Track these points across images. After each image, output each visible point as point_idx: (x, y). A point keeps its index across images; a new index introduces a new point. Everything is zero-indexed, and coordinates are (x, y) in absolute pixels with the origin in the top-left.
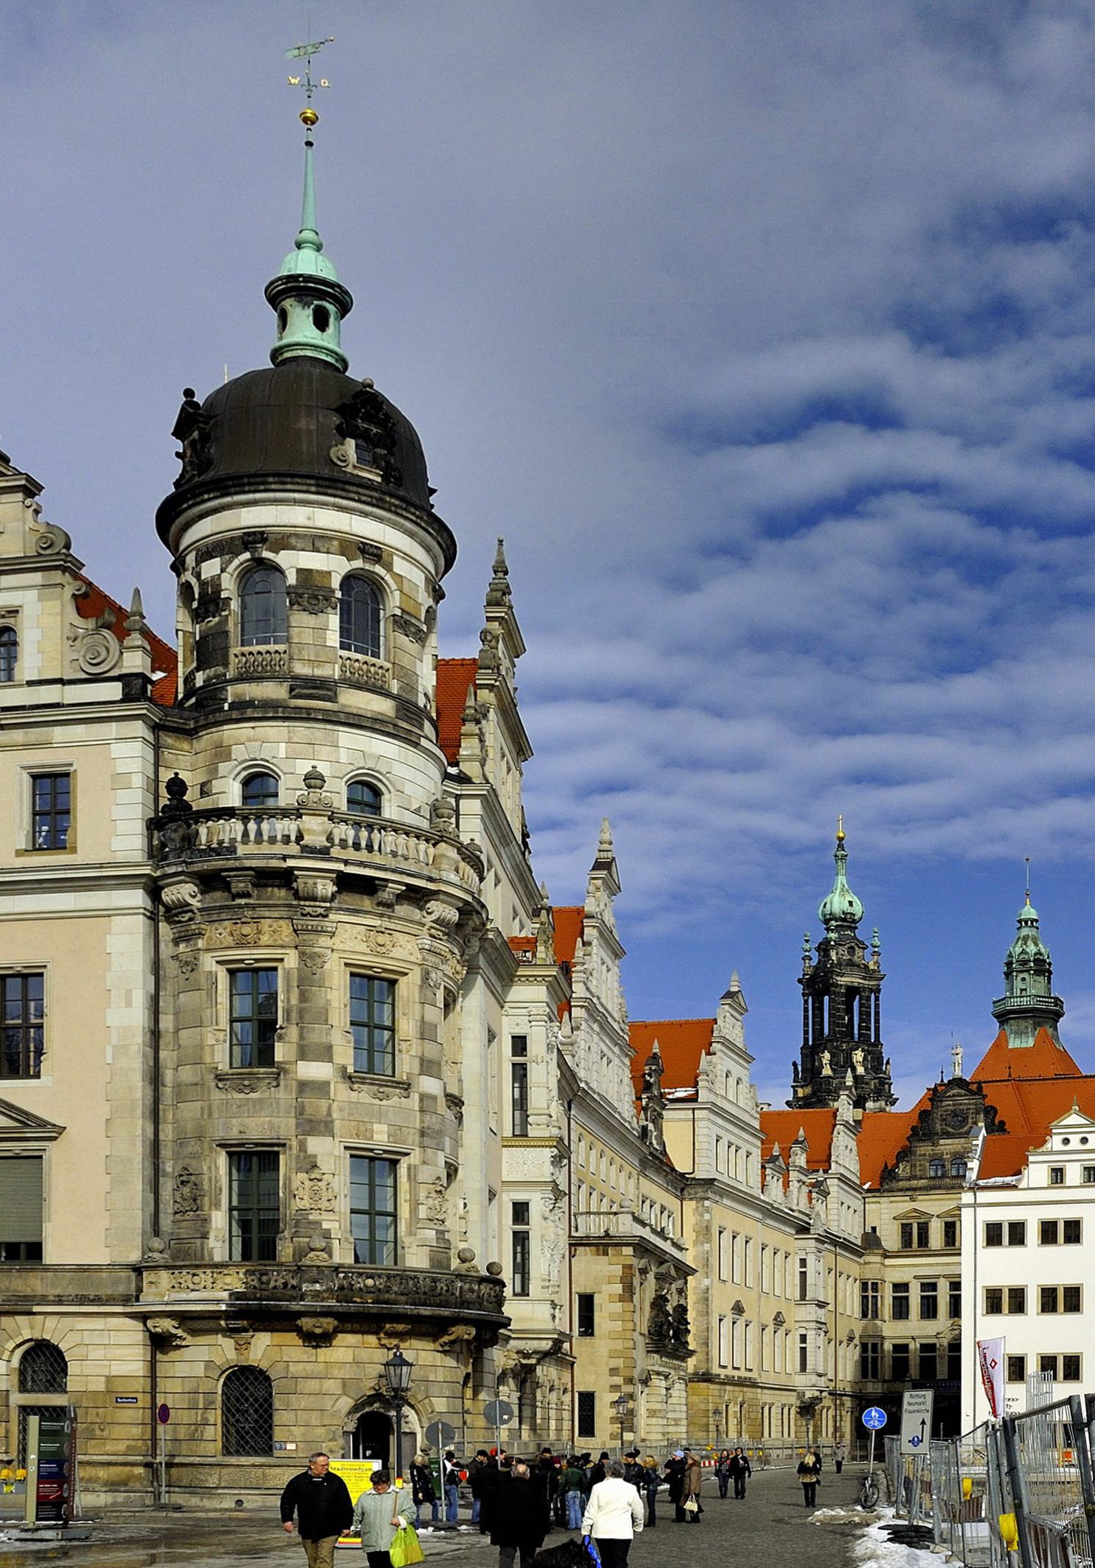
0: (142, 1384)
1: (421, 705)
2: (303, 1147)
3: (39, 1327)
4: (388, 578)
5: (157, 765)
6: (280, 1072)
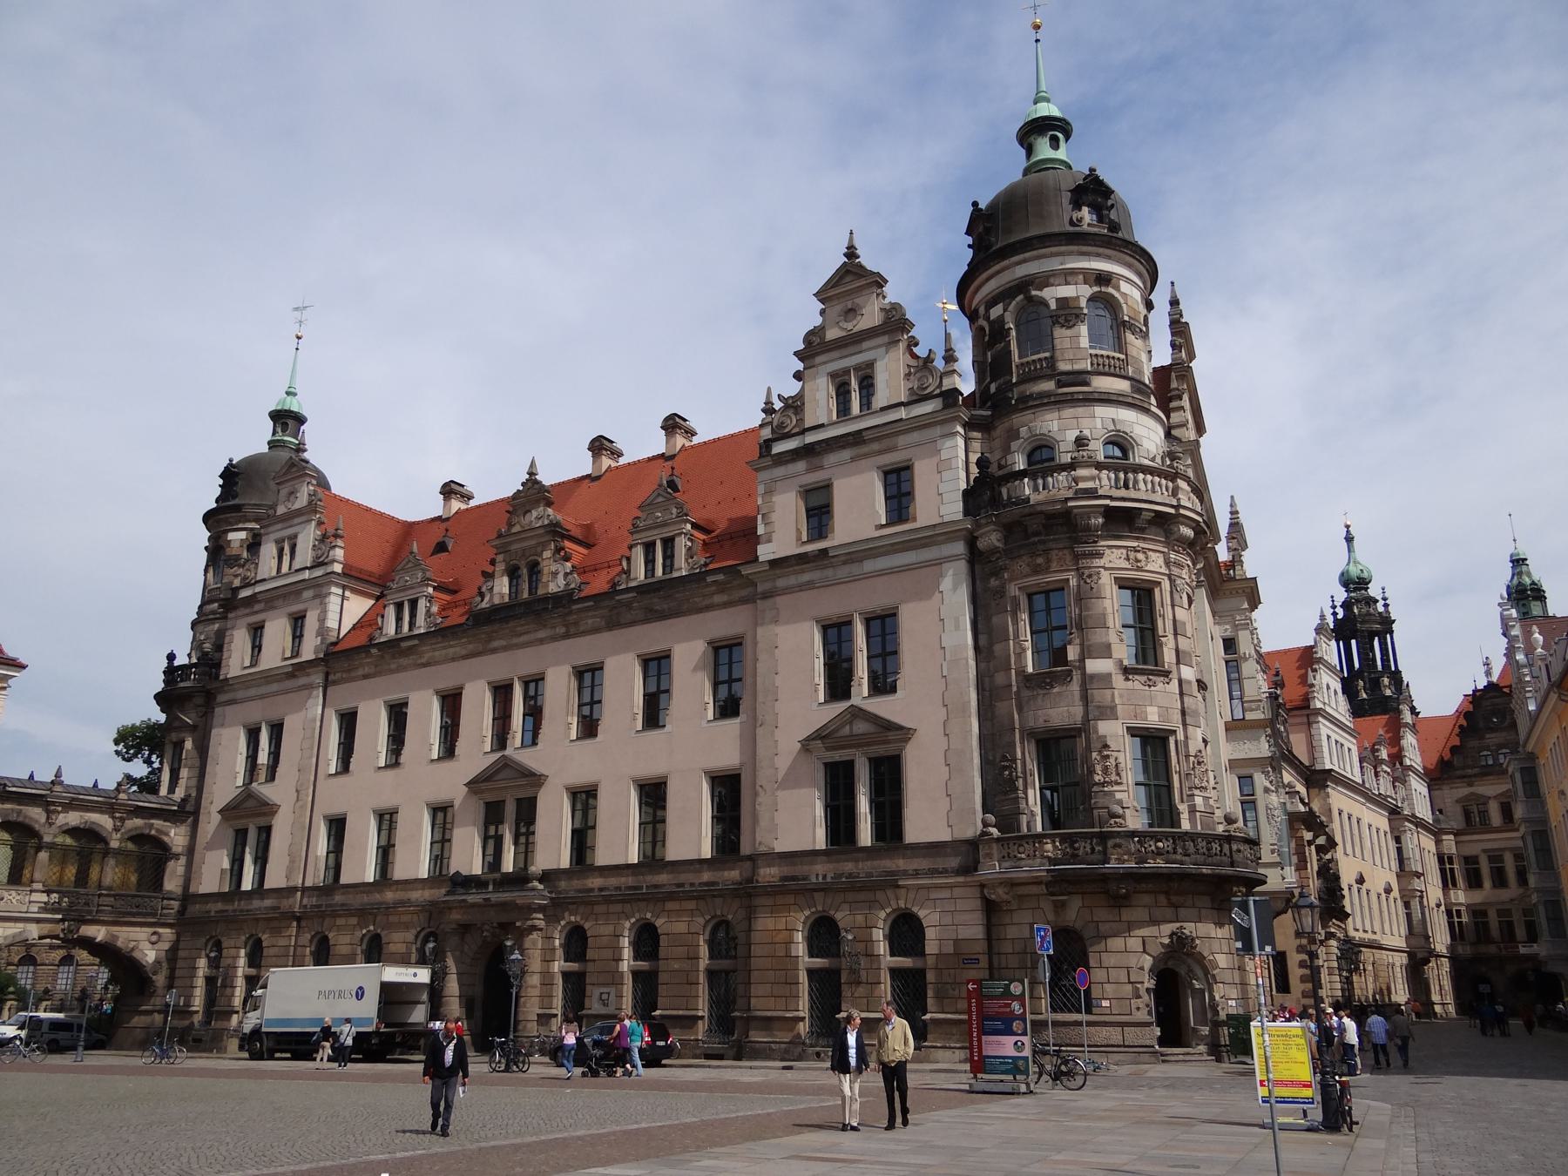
0: (981, 947)
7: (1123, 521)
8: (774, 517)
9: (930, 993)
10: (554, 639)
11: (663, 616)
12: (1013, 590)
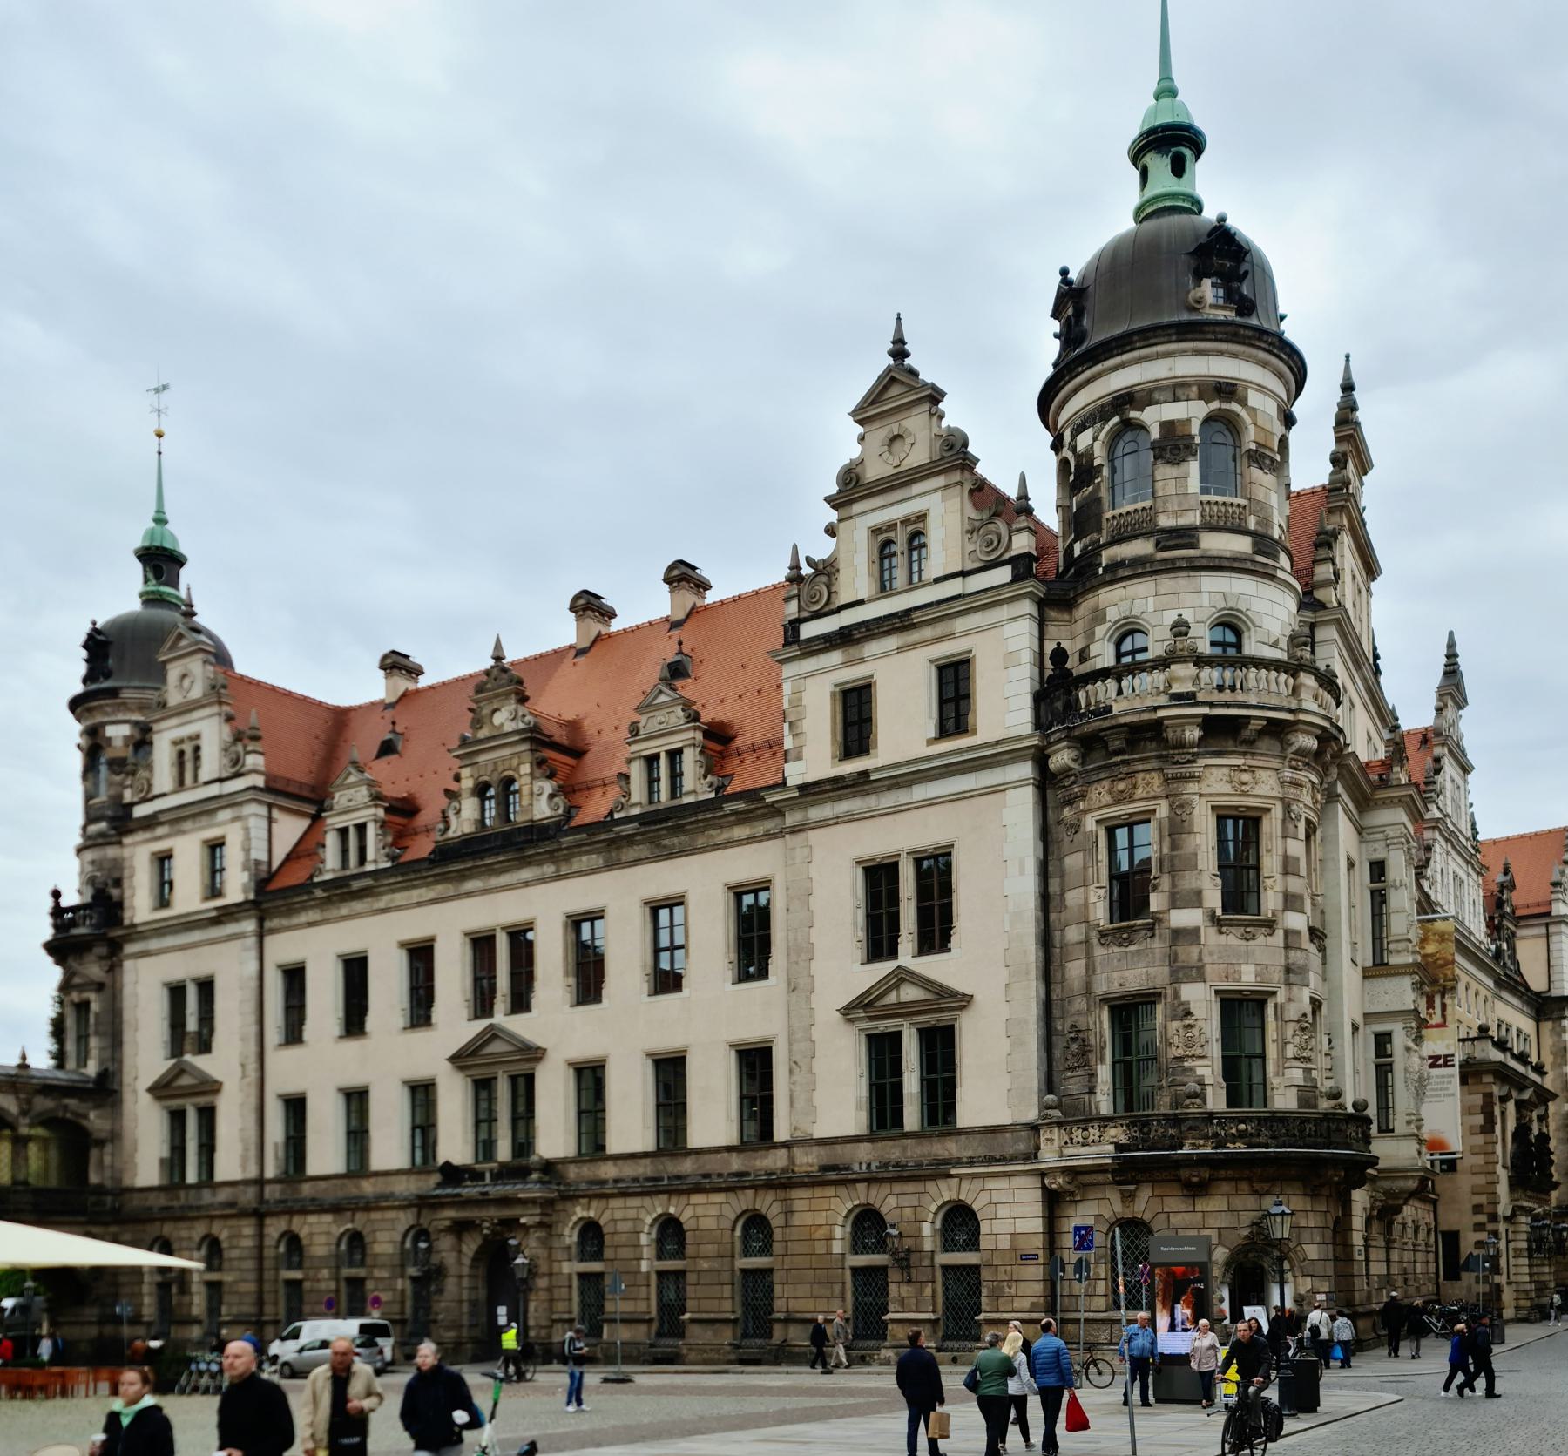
0: (1039, 1242)
1: (1276, 536)
2: (1176, 995)
3: (955, 1189)
4: (1243, 414)
5: (1041, 639)
6: (1154, 924)
7: (1223, 732)
8: (805, 726)
9: (984, 1292)
10: (542, 880)
11: (672, 855)
12: (1090, 824)
